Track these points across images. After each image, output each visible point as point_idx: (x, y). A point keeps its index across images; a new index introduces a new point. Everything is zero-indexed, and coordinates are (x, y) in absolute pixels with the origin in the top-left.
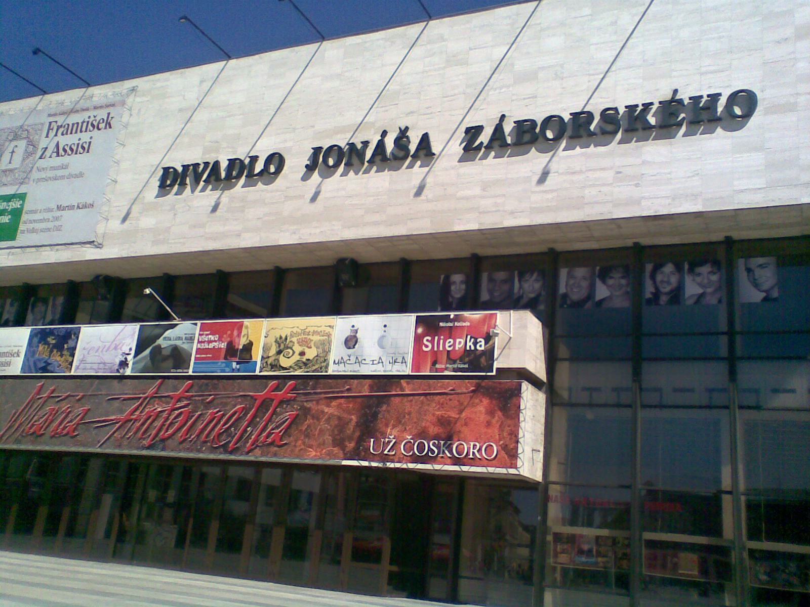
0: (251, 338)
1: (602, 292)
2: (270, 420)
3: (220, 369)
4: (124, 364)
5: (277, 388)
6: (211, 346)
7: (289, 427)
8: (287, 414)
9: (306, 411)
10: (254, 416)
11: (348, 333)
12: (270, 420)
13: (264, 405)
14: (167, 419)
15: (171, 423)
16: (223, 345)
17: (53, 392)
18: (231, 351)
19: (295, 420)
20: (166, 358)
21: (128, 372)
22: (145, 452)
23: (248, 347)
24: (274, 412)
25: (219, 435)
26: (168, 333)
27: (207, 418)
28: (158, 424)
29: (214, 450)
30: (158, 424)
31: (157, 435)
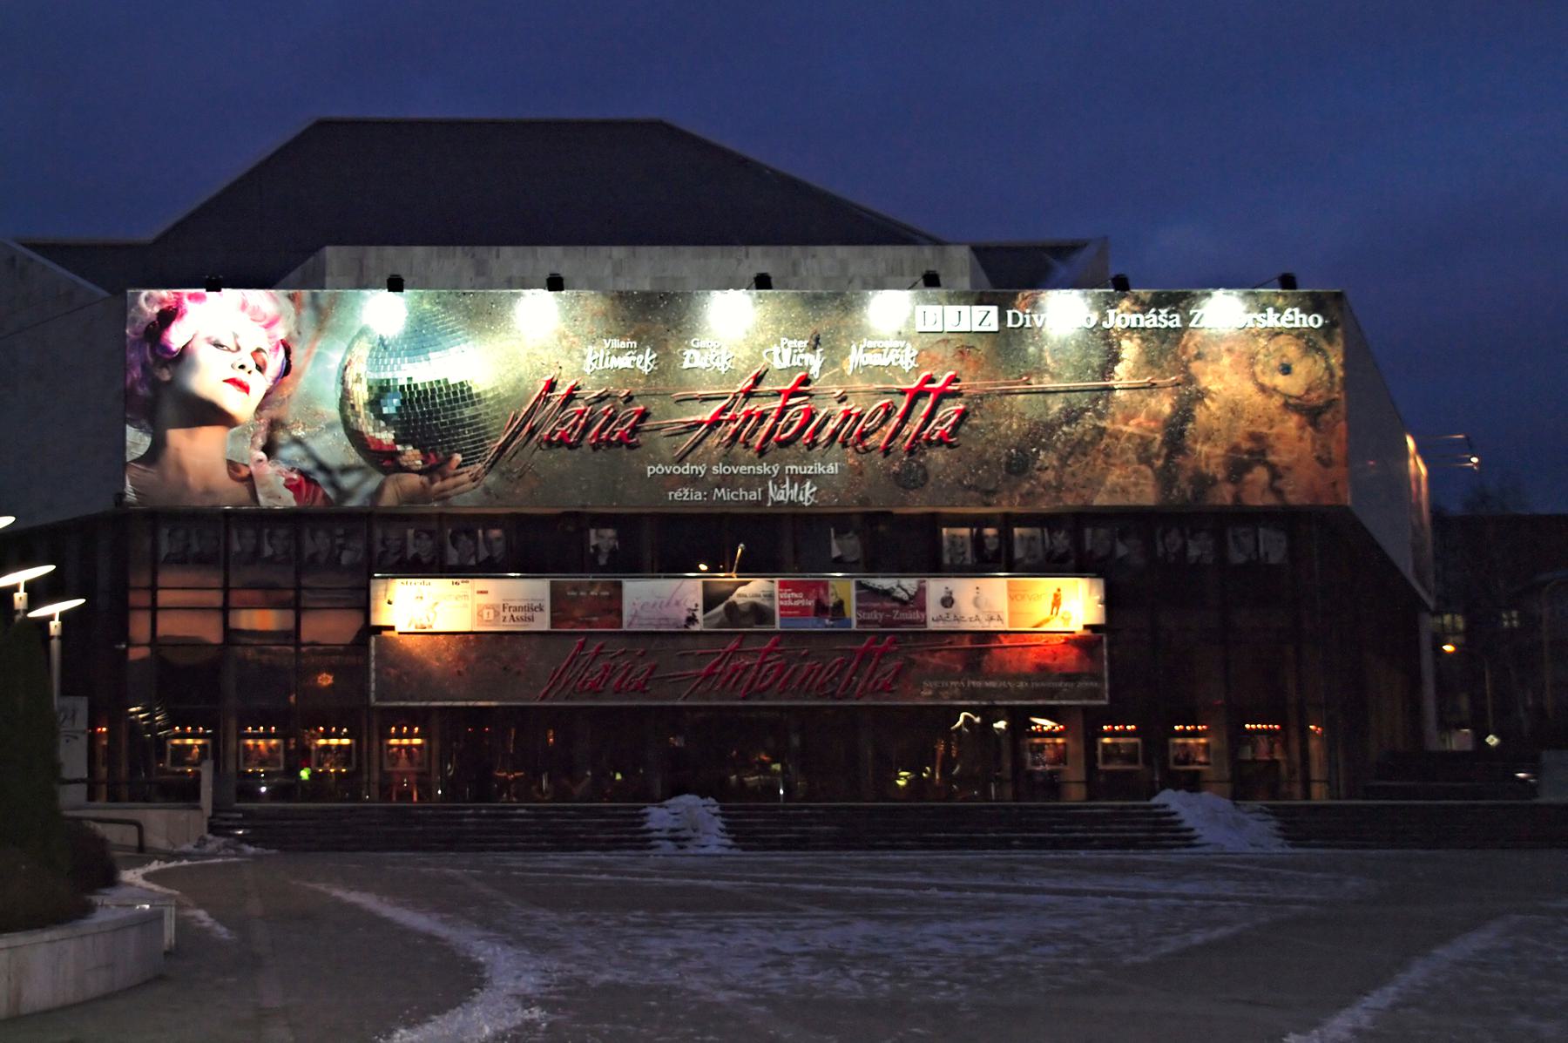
0: (841, 596)
2: (875, 670)
3: (813, 625)
4: (692, 620)
5: (873, 642)
6: (797, 603)
7: (897, 674)
8: (892, 665)
9: (912, 663)
10: (856, 669)
11: (943, 594)
12: (875, 670)
13: (865, 656)
14: (758, 672)
15: (765, 676)
16: (811, 603)
17: (602, 647)
18: (821, 609)
19: (899, 672)
20: (745, 615)
21: (696, 628)
22: (740, 703)
23: (840, 605)
24: (878, 663)
25: (823, 685)
26: (741, 590)
27: (805, 670)
28: (749, 676)
29: (819, 697)
30: (749, 676)
31: (750, 687)
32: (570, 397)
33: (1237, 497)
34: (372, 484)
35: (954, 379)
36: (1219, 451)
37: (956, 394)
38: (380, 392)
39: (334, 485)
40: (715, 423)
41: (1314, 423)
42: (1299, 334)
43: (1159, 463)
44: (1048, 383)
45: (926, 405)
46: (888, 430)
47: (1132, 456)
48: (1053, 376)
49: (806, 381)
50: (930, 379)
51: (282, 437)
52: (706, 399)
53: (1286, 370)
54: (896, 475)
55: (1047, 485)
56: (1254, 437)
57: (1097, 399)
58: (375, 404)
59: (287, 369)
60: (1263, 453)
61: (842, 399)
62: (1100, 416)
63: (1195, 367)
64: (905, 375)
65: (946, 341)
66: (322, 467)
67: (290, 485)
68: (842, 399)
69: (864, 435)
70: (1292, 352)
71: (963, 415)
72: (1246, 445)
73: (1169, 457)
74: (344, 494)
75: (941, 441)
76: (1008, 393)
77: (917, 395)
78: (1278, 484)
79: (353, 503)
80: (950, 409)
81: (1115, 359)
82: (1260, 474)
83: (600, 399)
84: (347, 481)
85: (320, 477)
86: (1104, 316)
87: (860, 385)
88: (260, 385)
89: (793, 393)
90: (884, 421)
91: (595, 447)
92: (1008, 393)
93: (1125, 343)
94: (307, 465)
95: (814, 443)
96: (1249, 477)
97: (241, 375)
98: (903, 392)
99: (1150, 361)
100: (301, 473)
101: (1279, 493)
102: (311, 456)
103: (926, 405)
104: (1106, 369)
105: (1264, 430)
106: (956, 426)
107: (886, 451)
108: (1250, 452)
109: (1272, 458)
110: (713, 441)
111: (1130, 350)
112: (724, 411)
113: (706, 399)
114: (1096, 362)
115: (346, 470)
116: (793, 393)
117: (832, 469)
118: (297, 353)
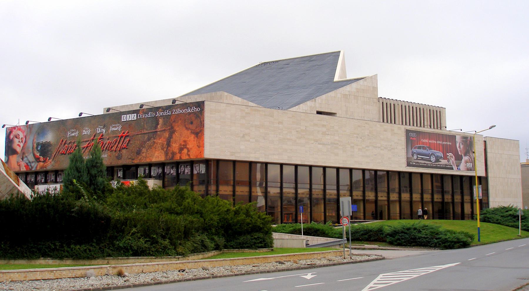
1: (172, 172)
32: (65, 143)
33: (180, 158)
34: (36, 165)
35: (128, 132)
36: (177, 146)
37: (128, 136)
38: (38, 144)
39: (31, 165)
40: (87, 147)
41: (197, 137)
42: (194, 113)
43: (165, 149)
44: (145, 132)
45: (123, 139)
46: (116, 146)
47: (160, 148)
48: (146, 129)
49: (102, 136)
50: (124, 133)
51: (24, 156)
52: (86, 141)
53: (192, 123)
54: (117, 157)
55: (144, 157)
56: (185, 141)
57: (153, 135)
58: (37, 148)
59: (25, 142)
60: (186, 145)
61: (108, 139)
62: (154, 139)
63: (174, 124)
64: (119, 132)
65: (127, 123)
66: (30, 162)
67: (25, 166)
68: (108, 139)
69: (112, 147)
70: (193, 118)
71: (129, 141)
72: (183, 143)
73: (167, 148)
74: (32, 167)
75: (125, 148)
76: (138, 135)
77: (122, 137)
78: (189, 153)
79: (33, 169)
80: (127, 139)
81: (158, 124)
82: (185, 151)
83: (70, 143)
84: (33, 164)
85: (29, 164)
86: (156, 114)
87: (111, 136)
88: (22, 145)
89: (100, 139)
90: (115, 144)
91: (68, 154)
92: (138, 135)
93: (160, 120)
94: (27, 162)
95: (103, 150)
96: (183, 152)
97: (19, 143)
98: (119, 136)
99: (164, 124)
100: (27, 163)
101: (189, 155)
102: (28, 160)
103: (123, 139)
104: (156, 127)
105: (187, 139)
106: (128, 144)
107: (115, 151)
108: (184, 145)
109: (188, 146)
110: (87, 151)
111: (161, 121)
112: (88, 144)
113: (86, 141)
114: (154, 125)
115: (33, 162)
116: (100, 139)
117: (106, 156)
118: (27, 138)
